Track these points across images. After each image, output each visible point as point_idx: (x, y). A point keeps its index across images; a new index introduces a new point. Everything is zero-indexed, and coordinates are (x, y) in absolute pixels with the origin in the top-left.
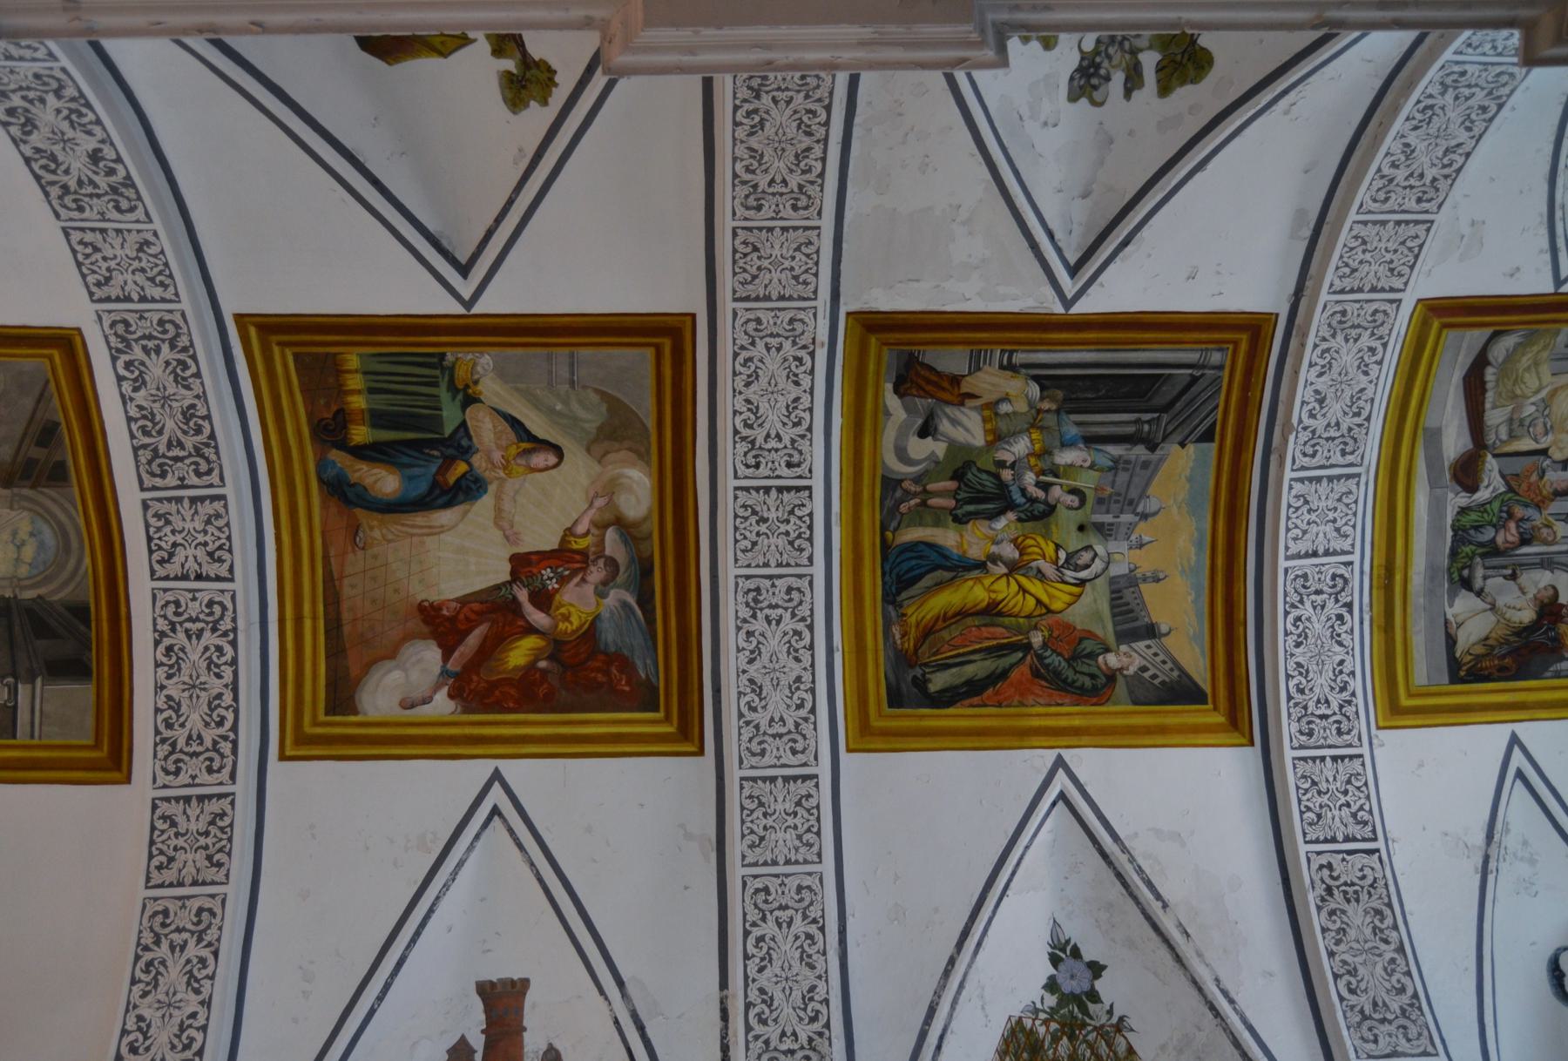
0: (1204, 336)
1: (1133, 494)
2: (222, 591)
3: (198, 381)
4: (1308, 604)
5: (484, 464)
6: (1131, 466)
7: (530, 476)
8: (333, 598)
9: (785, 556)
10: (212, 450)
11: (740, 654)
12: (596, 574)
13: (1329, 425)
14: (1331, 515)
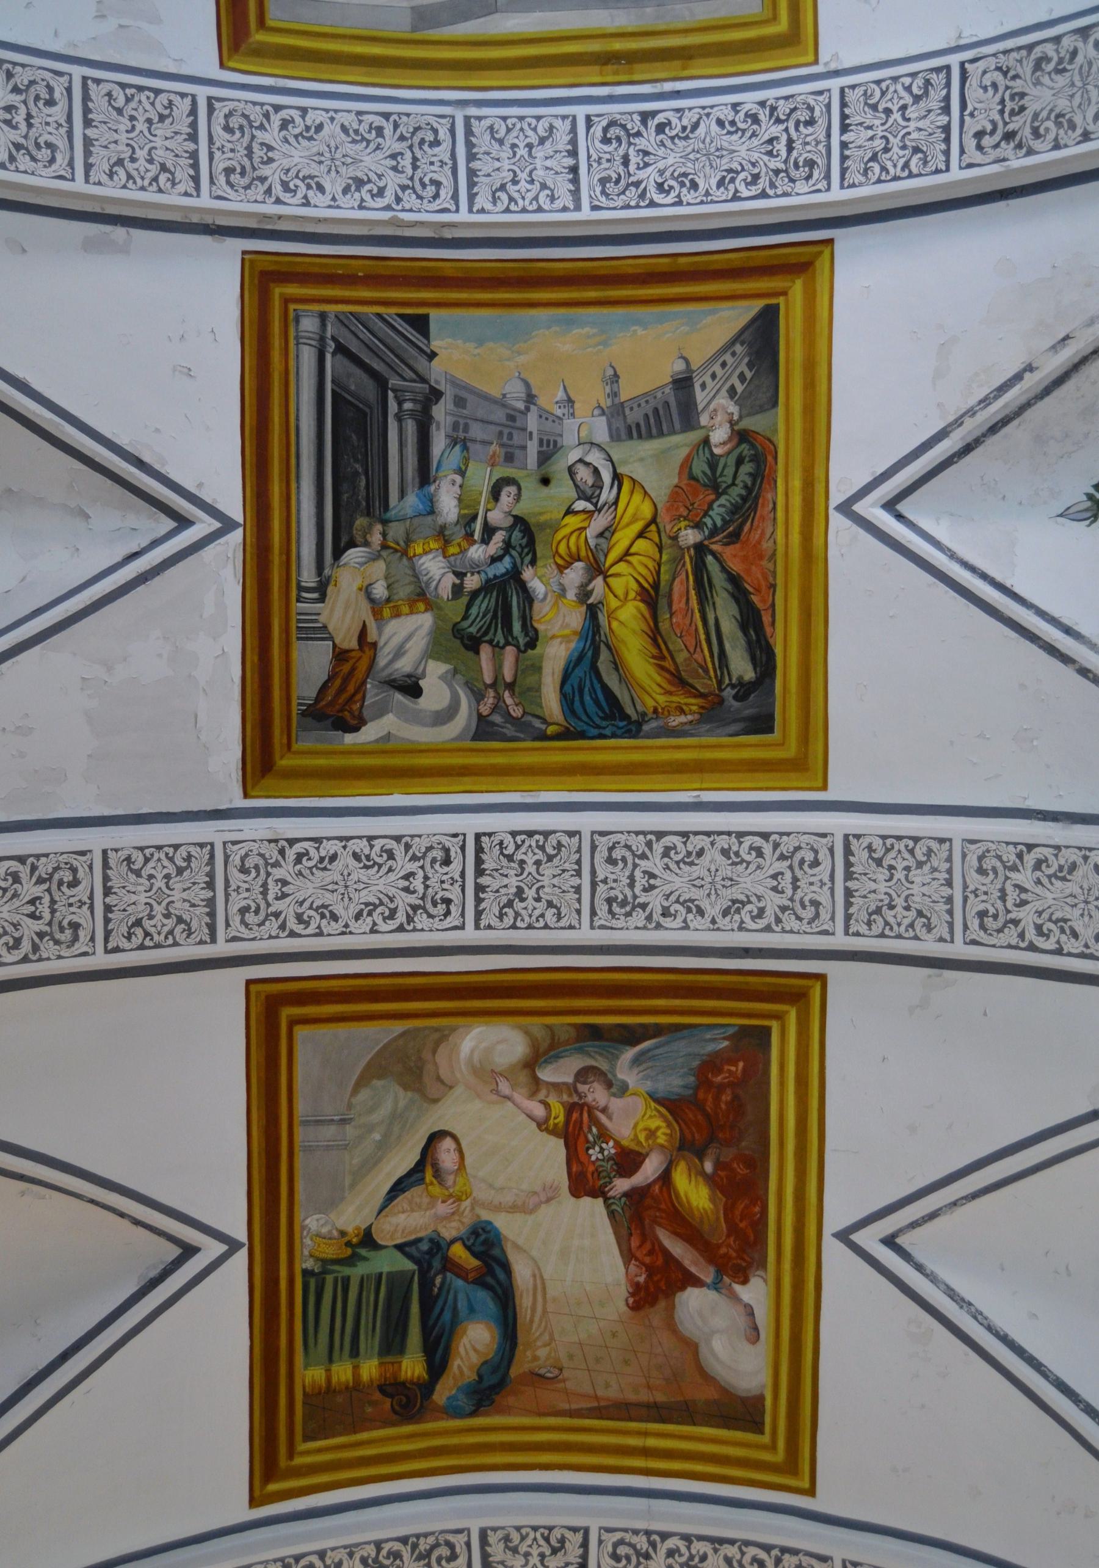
0: (276, 342)
1: (499, 415)
2: (600, 1542)
3: (329, 1553)
4: (641, 175)
5: (454, 1224)
6: (462, 421)
7: (468, 1171)
8: (622, 1410)
9: (567, 866)
10: (422, 1540)
11: (691, 925)
12: (596, 1094)
13: (395, 169)
14: (522, 152)
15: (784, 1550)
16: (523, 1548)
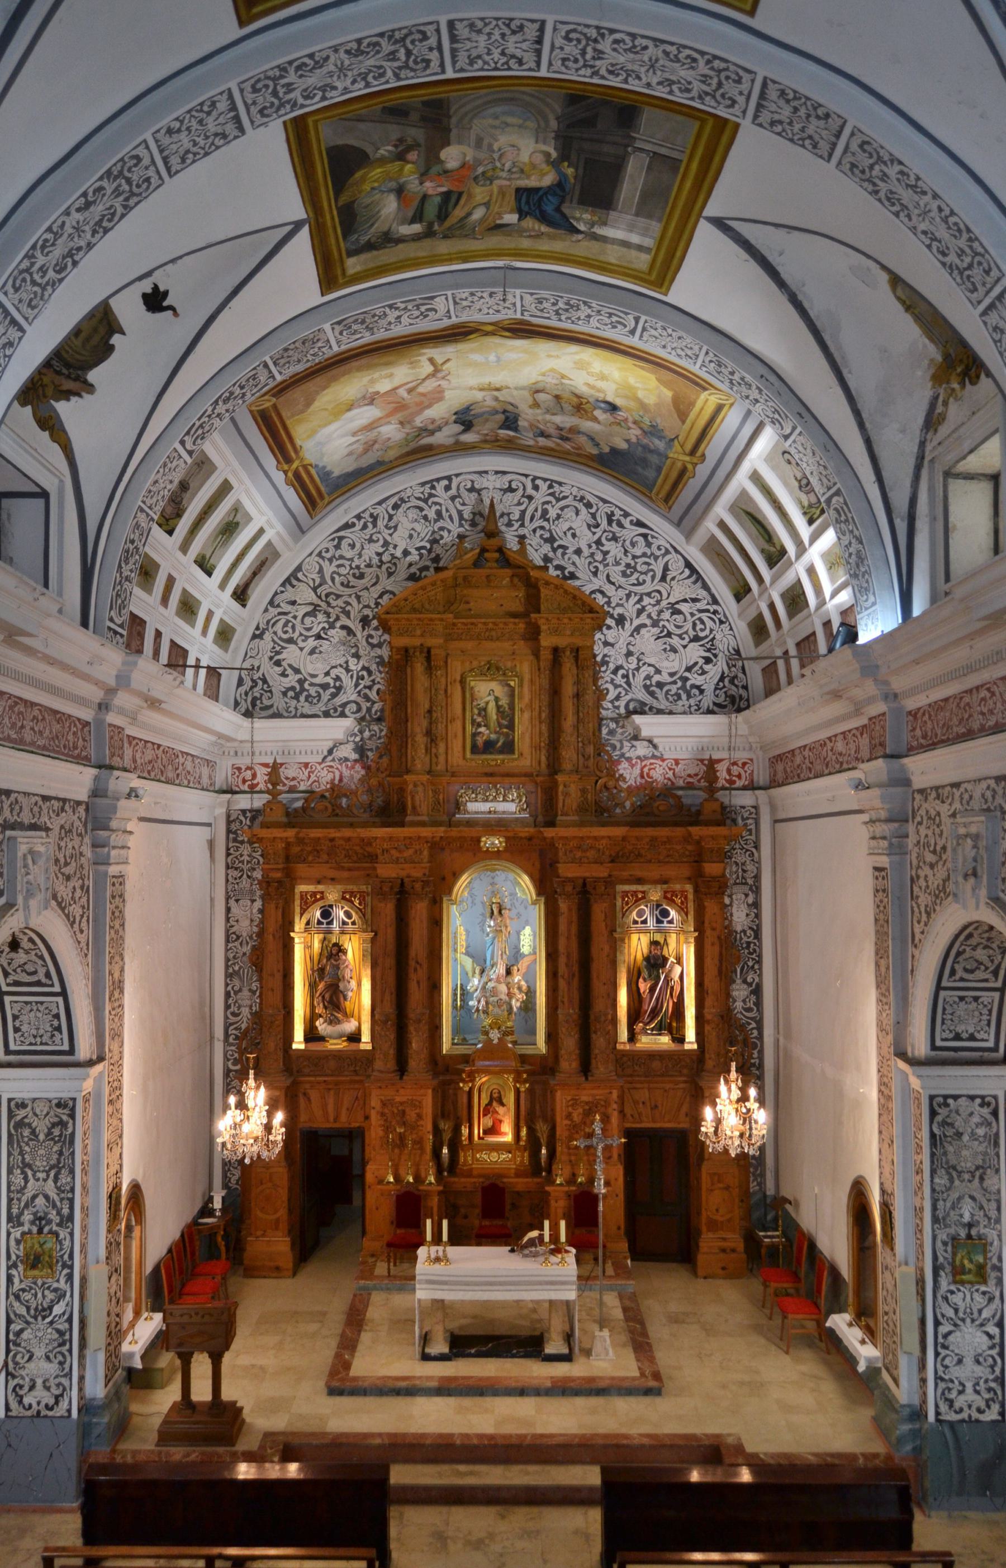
15: (715, 57)
16: (487, 30)
